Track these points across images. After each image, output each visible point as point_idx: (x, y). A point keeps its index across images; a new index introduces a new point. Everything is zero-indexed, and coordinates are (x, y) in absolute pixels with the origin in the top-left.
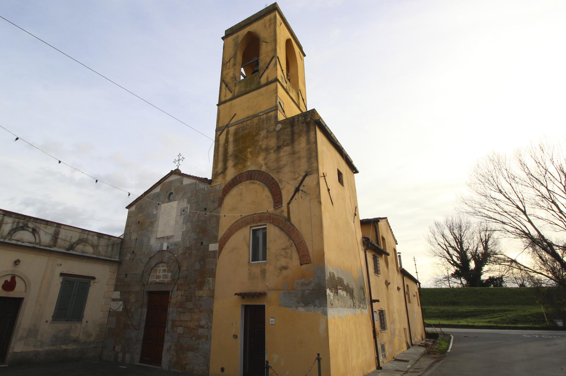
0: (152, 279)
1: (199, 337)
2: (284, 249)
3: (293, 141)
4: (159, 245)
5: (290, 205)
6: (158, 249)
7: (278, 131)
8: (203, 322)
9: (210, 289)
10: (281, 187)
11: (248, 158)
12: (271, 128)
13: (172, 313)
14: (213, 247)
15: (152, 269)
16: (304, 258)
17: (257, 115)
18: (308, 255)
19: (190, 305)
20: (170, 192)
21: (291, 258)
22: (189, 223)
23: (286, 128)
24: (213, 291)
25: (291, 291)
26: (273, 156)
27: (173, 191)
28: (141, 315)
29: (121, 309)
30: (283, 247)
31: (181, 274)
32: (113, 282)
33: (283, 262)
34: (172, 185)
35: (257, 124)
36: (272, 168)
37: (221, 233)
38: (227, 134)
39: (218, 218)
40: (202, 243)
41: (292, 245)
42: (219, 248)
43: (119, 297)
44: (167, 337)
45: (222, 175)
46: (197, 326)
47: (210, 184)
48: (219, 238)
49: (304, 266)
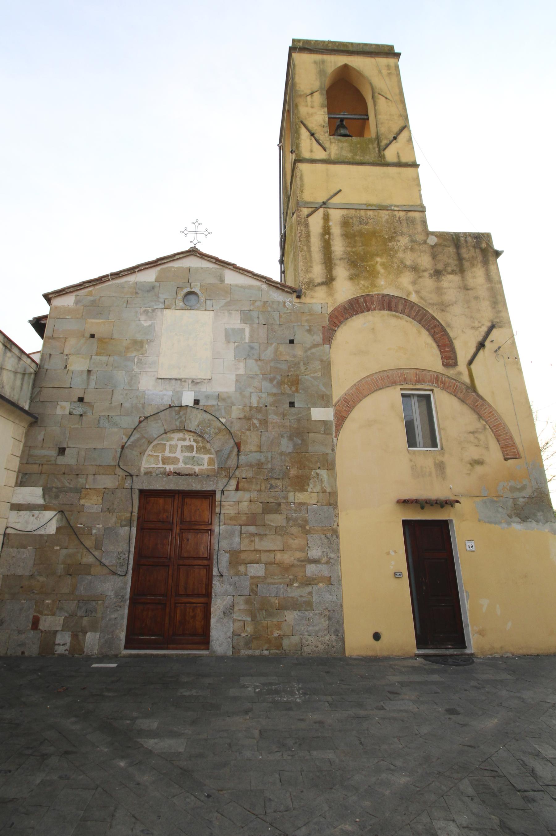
0: (150, 462)
1: (309, 582)
2: (473, 433)
3: (461, 270)
4: (170, 393)
5: (472, 366)
6: (167, 401)
7: (433, 247)
8: (315, 553)
9: (324, 491)
10: (451, 334)
11: (378, 273)
12: (420, 238)
13: (225, 538)
14: (320, 414)
15: (150, 442)
16: (510, 451)
17: (387, 206)
18: (514, 445)
19: (276, 520)
20: (188, 290)
21: (487, 448)
22: (251, 362)
23: (446, 246)
24: (333, 494)
25: (495, 499)
26: (428, 283)
27: (197, 290)
28: (122, 544)
29: (52, 529)
30: (471, 429)
31: (242, 458)
32: (15, 464)
33: (473, 453)
34: (186, 278)
35: (387, 222)
36: (431, 301)
37: (338, 392)
38: (326, 218)
39: (326, 366)
40: (292, 404)
41: (485, 429)
42: (336, 415)
43: (41, 501)
44: (218, 586)
45: (324, 288)
46: (299, 560)
47: (298, 297)
48: (335, 400)
49: (509, 461)
